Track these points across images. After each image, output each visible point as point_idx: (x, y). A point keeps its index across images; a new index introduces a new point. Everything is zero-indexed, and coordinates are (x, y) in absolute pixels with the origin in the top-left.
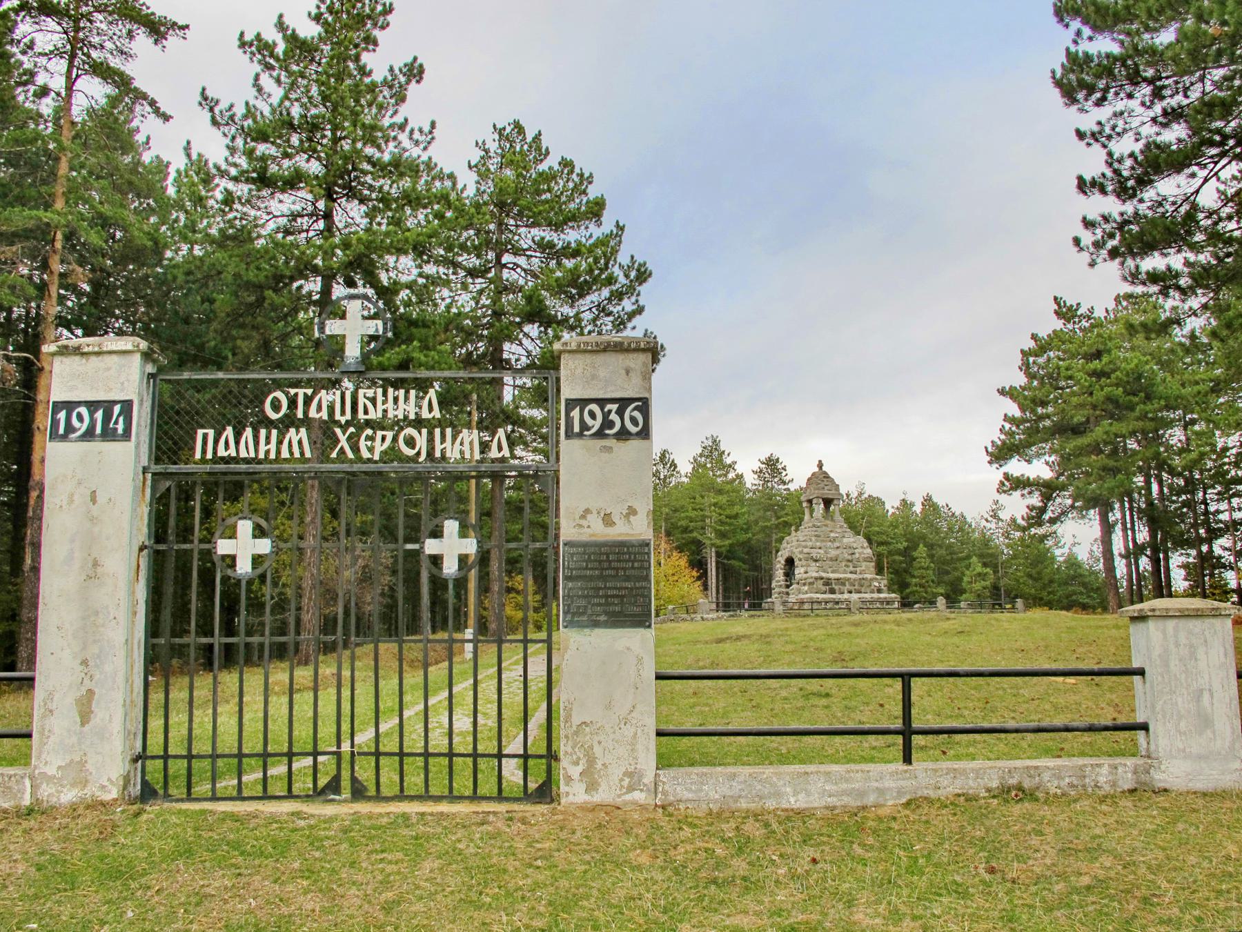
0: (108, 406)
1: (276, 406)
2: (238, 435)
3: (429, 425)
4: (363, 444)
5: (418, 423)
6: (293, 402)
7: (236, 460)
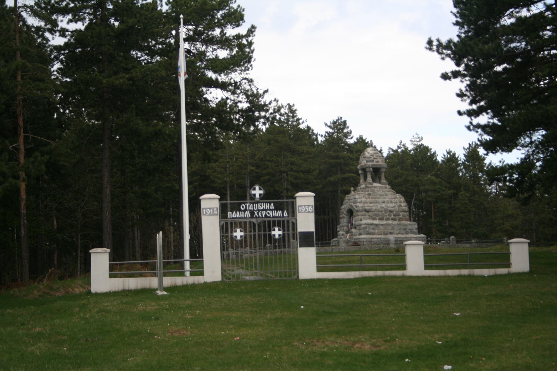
0: (213, 208)
1: (243, 207)
2: (236, 213)
3: (272, 210)
4: (260, 214)
5: (270, 210)
6: (246, 206)
7: (236, 218)
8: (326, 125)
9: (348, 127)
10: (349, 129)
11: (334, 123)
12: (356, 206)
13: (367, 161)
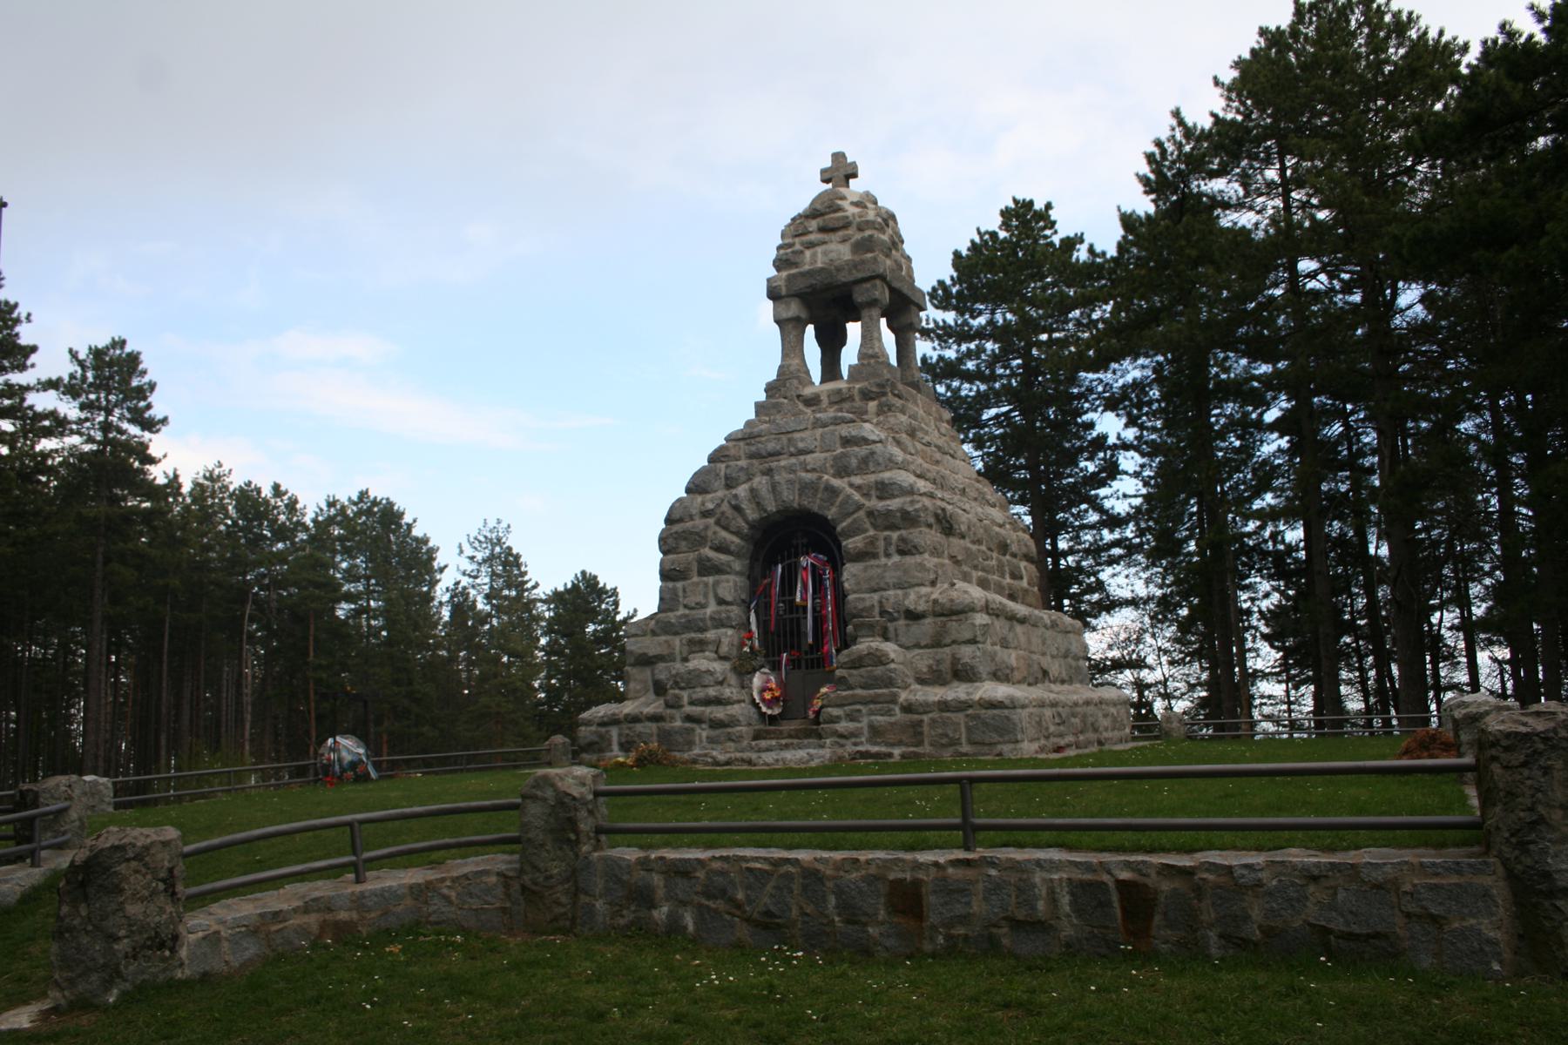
8: (73, 354)
9: (144, 372)
10: (146, 379)
11: (97, 353)
12: (884, 490)
13: (859, 247)
